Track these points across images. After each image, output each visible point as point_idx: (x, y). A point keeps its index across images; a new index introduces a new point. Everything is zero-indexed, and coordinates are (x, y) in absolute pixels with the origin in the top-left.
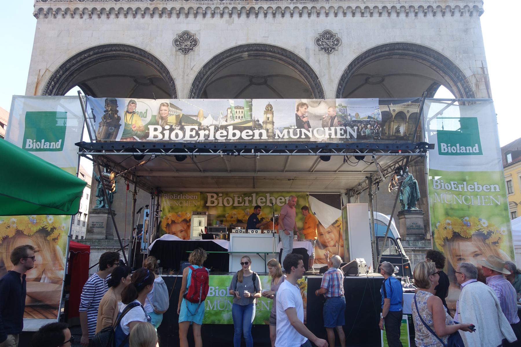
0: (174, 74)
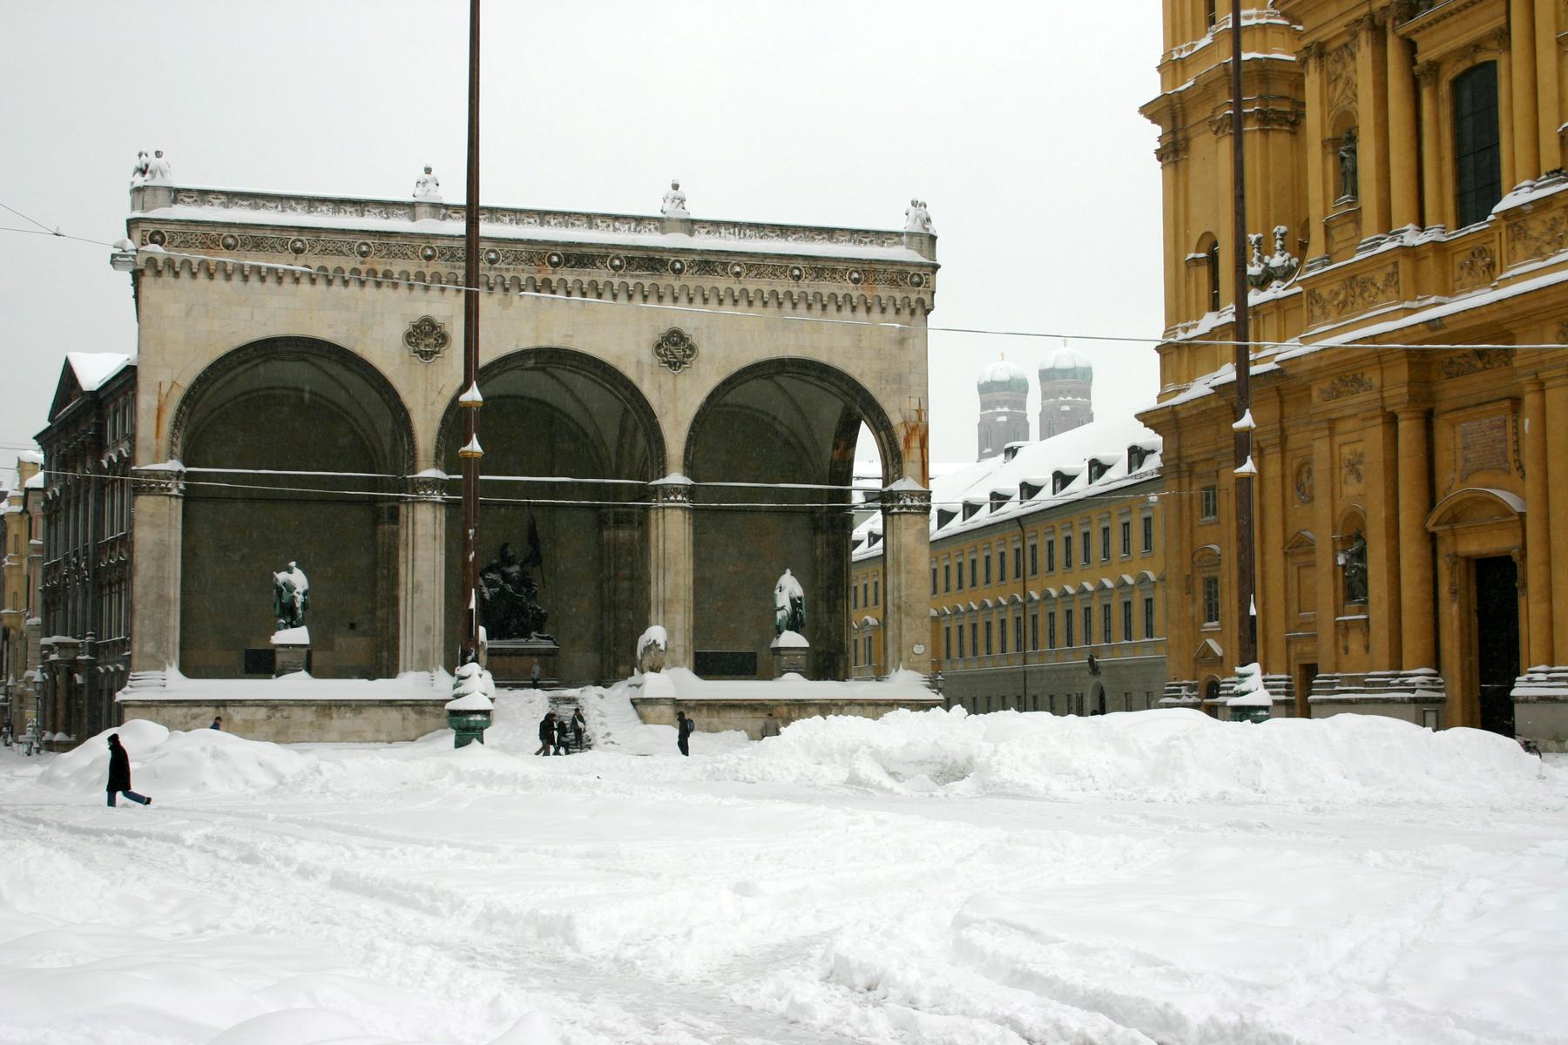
0: (408, 399)
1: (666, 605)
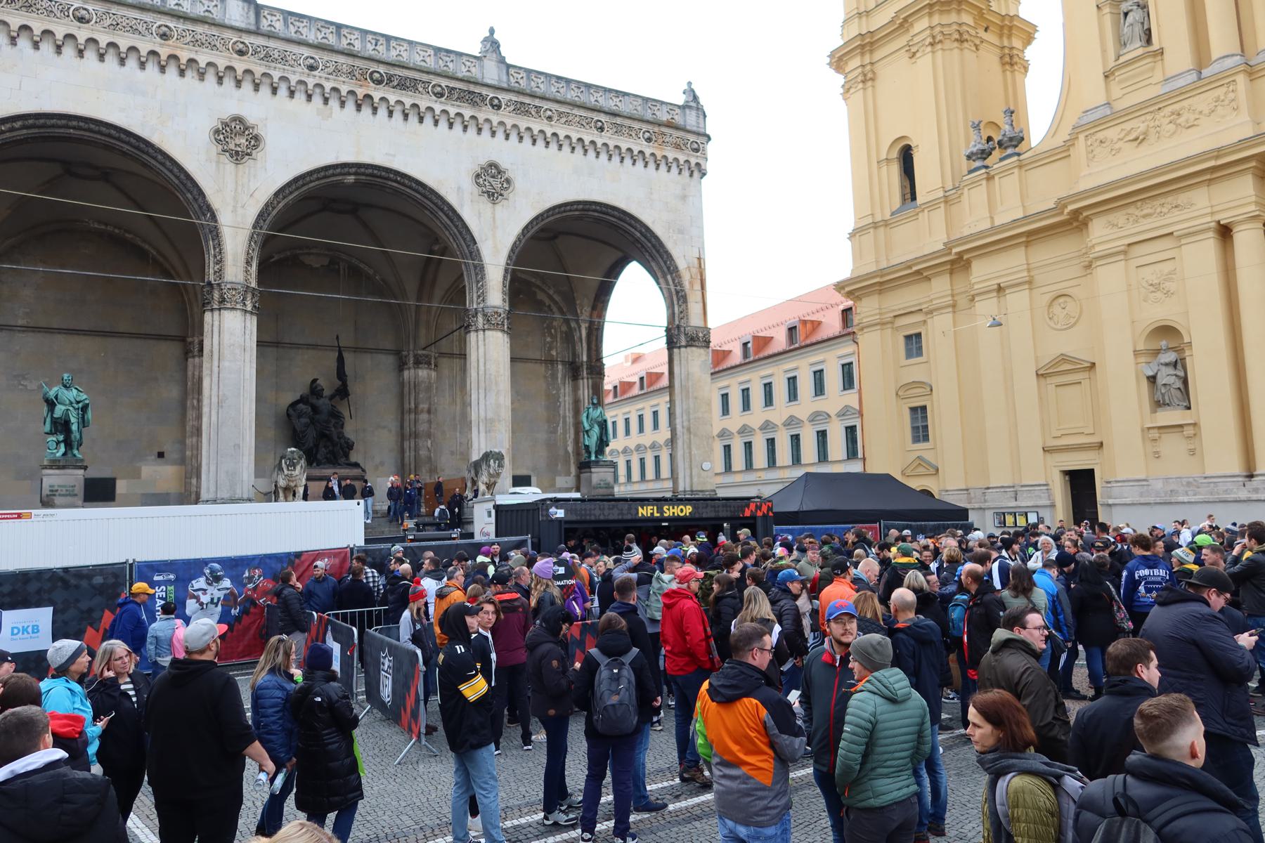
1: (490, 423)
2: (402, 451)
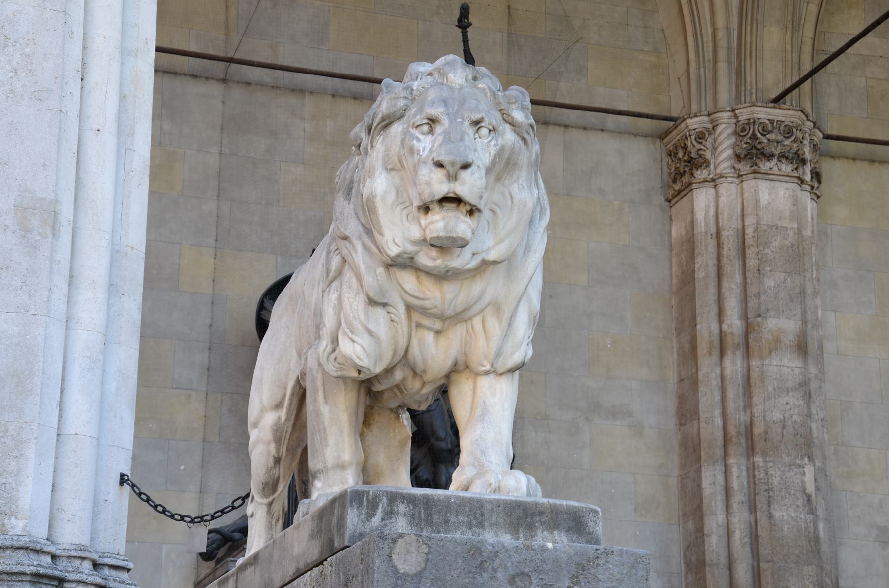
2: (693, 509)
